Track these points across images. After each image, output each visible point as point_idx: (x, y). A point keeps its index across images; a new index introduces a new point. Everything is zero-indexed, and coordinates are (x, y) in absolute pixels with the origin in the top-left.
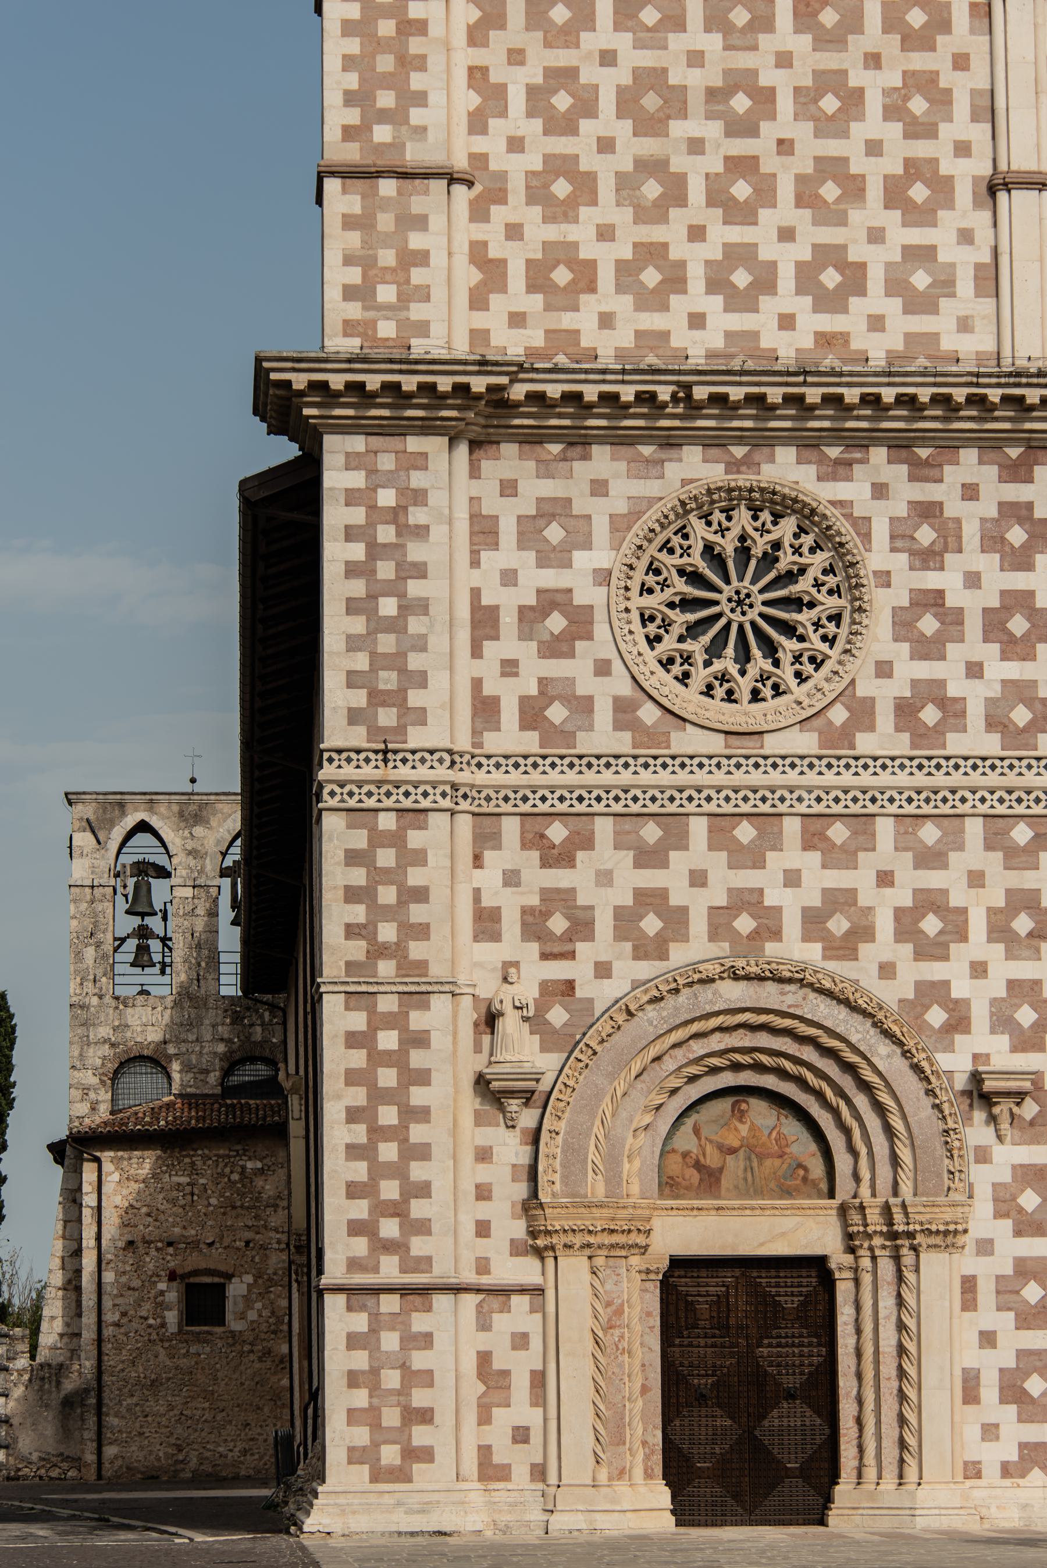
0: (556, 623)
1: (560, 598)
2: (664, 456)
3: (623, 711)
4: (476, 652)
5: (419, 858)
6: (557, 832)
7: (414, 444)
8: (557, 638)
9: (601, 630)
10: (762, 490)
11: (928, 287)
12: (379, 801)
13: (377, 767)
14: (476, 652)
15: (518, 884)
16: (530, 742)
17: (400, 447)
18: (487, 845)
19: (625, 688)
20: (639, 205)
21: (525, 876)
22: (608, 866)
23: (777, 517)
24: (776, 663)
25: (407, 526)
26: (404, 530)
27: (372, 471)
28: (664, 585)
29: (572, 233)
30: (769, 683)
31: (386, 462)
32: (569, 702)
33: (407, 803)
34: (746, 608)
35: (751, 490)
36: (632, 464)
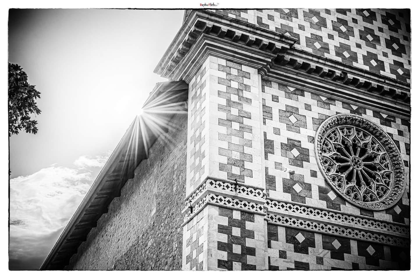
0: (295, 152)
1: (296, 143)
2: (330, 102)
3: (323, 192)
4: (266, 158)
5: (251, 234)
6: (300, 238)
7: (245, 68)
8: (296, 158)
9: (312, 159)
10: (363, 122)
11: (403, 74)
12: (233, 205)
13: (232, 190)
14: (266, 158)
15: (285, 258)
16: (287, 197)
17: (240, 68)
18: (272, 238)
19: (323, 185)
20: (311, 23)
21: (288, 254)
22: (321, 256)
23: (365, 135)
24: (370, 188)
25: (243, 97)
26: (240, 98)
27: (229, 74)
28: (330, 150)
29: (291, 24)
30: (369, 195)
31: (234, 72)
32: (302, 184)
33: (246, 209)
34: (358, 165)
35: (360, 122)
36: (319, 102)
